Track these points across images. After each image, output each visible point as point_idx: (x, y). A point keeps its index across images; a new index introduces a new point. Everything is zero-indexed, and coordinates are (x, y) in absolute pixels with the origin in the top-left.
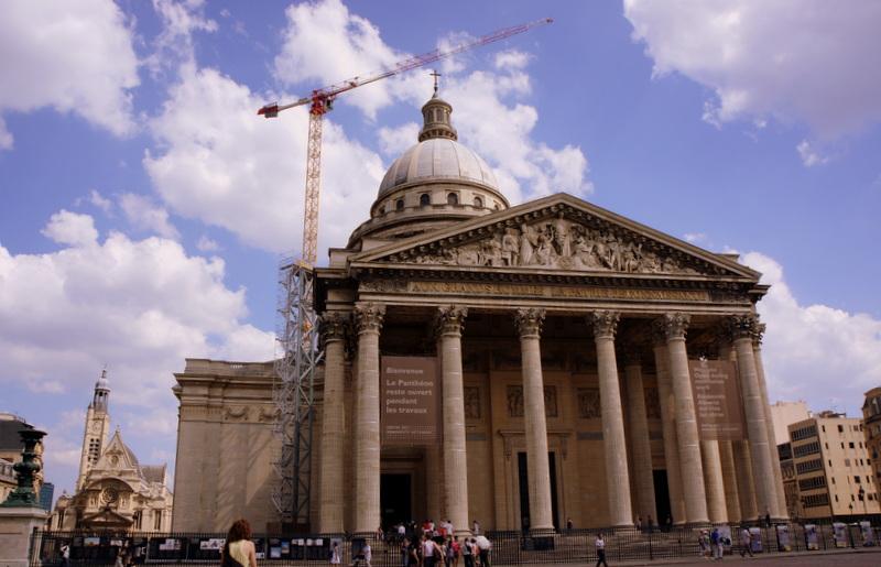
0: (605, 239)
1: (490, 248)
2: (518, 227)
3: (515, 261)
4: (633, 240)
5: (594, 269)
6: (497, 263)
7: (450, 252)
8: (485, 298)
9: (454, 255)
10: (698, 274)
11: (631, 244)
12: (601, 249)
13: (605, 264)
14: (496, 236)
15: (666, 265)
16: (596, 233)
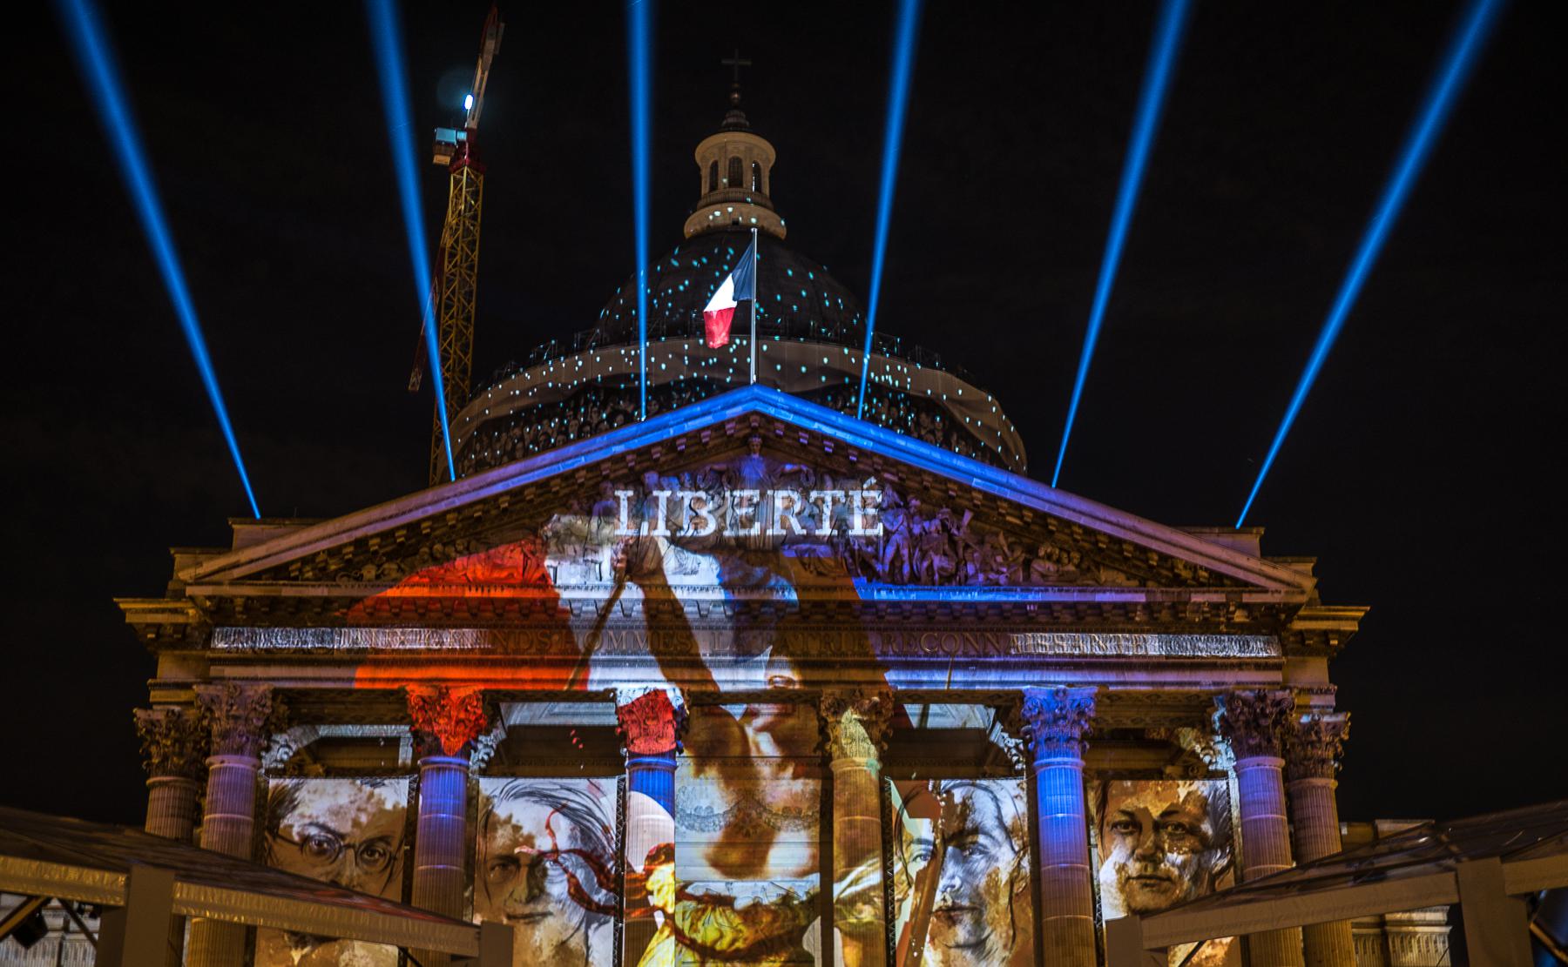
5: (826, 581)
7: (451, 550)
8: (533, 664)
10: (1134, 583)
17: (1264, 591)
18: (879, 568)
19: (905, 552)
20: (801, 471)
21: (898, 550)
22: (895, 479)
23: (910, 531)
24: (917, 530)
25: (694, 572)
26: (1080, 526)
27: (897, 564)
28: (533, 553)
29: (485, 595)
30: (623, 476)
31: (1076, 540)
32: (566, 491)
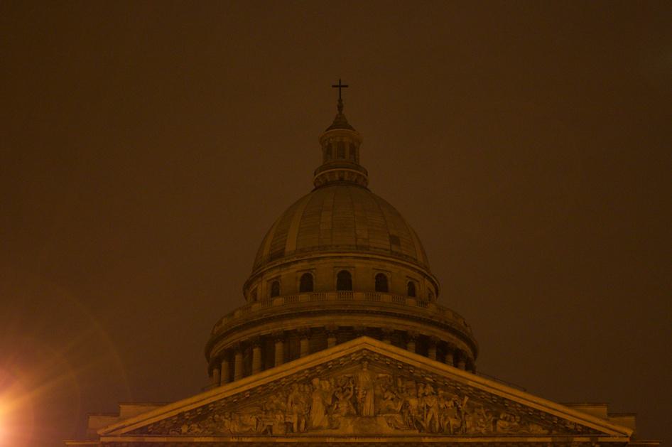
0: (421, 390)
1: (272, 409)
2: (308, 381)
3: (302, 426)
4: (457, 391)
5: (399, 432)
6: (278, 430)
7: (222, 417)
9: (227, 422)
10: (546, 432)
11: (455, 397)
12: (413, 402)
13: (421, 429)
14: (280, 393)
15: (500, 423)
16: (411, 384)
17: (609, 436)
18: (424, 425)
19: (437, 417)
20: (387, 377)
21: (433, 416)
22: (432, 380)
23: (439, 406)
24: (442, 406)
25: (336, 428)
26: (521, 404)
27: (433, 422)
28: (261, 418)
29: (240, 441)
30: (303, 380)
31: (518, 411)
32: (276, 388)
